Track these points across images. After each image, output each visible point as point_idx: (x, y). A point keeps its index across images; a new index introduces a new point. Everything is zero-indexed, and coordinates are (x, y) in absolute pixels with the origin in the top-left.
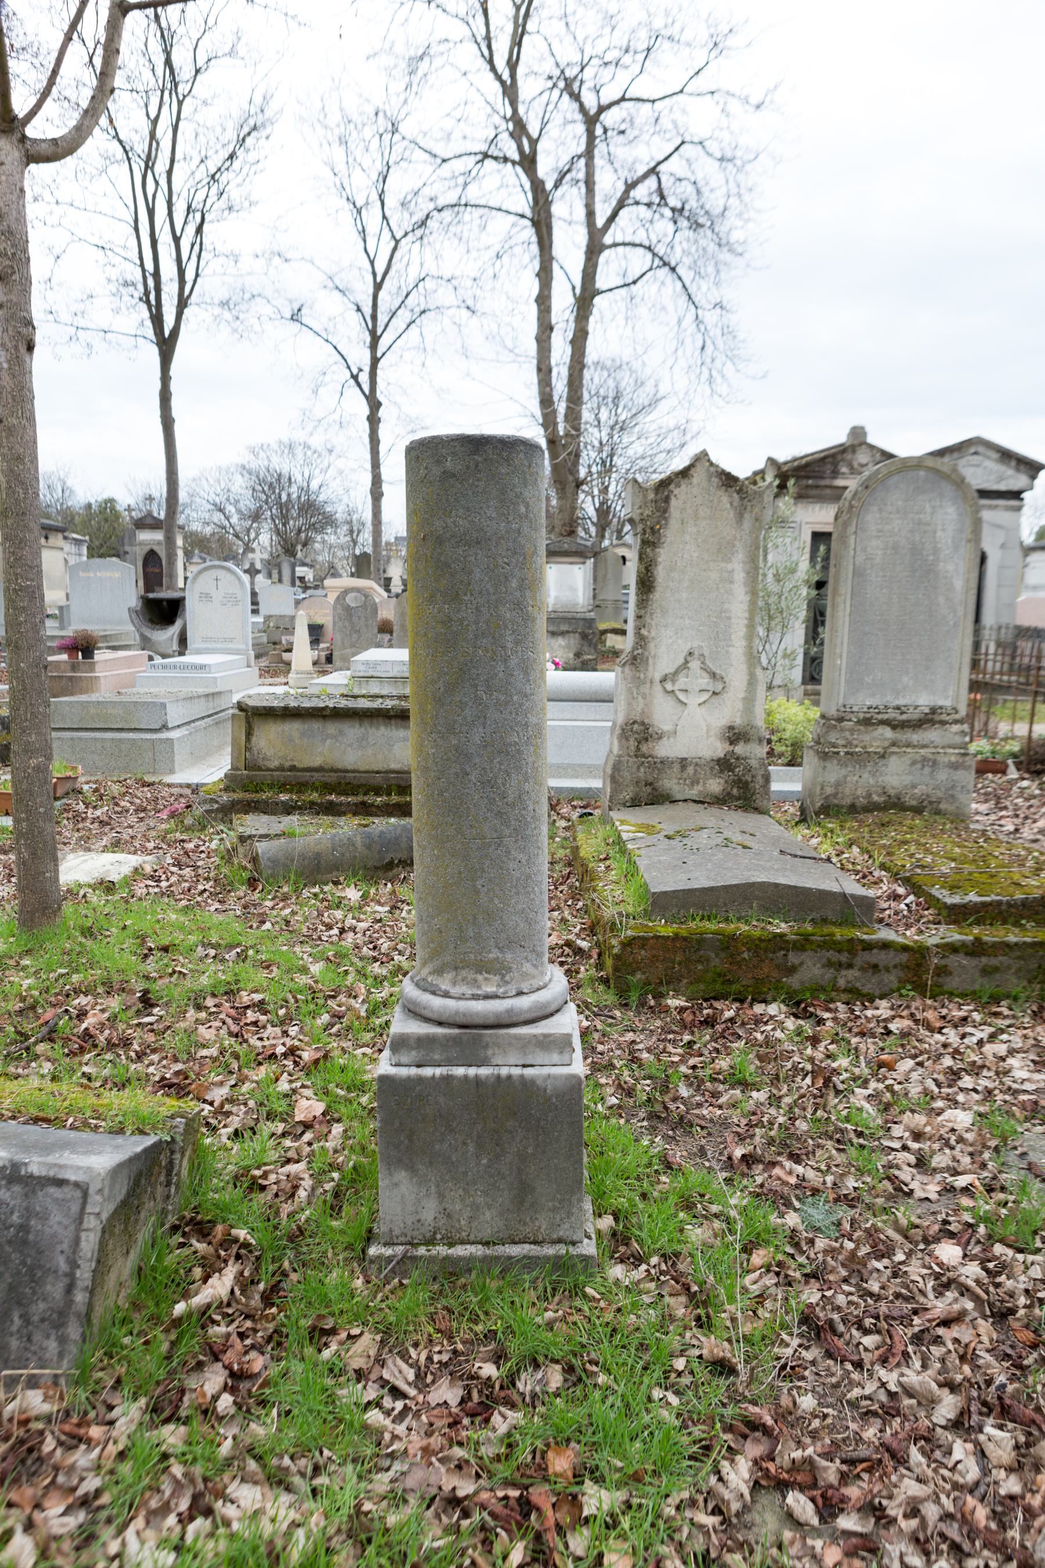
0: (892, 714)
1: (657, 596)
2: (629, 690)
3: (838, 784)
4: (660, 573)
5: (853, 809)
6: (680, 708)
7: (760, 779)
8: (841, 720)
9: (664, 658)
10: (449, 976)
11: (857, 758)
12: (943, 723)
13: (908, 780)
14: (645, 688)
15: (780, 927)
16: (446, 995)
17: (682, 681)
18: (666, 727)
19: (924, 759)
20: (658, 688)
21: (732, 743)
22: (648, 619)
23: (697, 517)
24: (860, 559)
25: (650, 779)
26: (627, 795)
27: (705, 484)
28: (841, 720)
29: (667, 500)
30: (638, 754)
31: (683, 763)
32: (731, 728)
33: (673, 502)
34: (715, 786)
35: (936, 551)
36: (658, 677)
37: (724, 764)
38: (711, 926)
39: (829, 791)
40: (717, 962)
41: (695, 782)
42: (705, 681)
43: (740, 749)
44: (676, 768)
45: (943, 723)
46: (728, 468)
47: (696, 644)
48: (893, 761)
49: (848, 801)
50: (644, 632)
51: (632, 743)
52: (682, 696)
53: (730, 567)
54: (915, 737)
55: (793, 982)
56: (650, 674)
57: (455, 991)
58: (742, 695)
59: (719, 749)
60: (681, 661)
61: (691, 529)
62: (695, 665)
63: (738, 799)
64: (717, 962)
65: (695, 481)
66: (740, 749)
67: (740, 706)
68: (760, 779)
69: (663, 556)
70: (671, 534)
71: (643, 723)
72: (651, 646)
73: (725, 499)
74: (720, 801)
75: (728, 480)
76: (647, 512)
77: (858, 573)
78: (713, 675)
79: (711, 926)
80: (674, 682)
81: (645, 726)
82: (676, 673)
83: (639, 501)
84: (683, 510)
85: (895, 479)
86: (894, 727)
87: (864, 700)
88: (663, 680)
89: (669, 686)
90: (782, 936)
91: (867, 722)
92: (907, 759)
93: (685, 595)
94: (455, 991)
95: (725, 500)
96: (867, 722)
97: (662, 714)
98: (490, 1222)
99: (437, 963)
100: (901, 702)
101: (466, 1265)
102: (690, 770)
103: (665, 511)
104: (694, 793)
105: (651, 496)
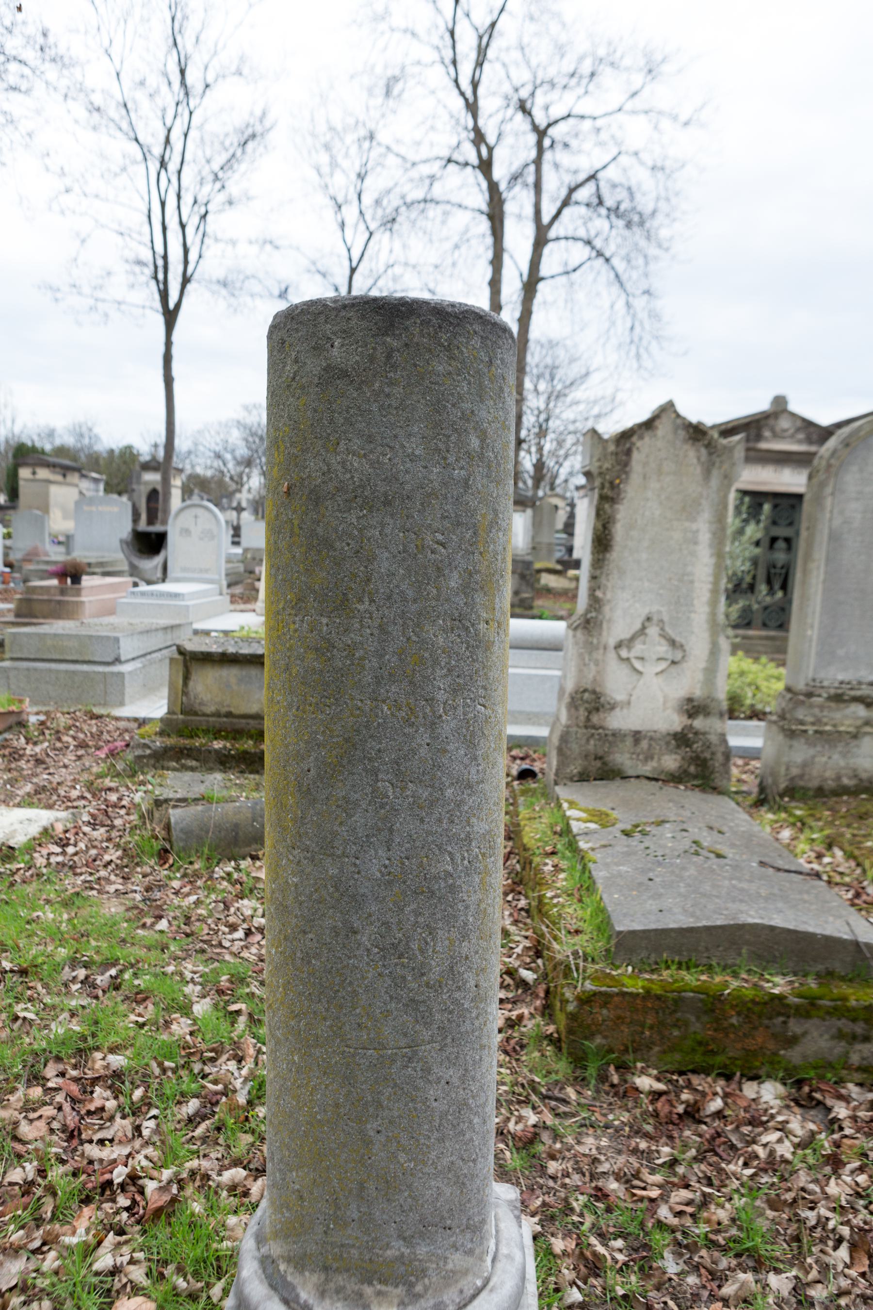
1: (614, 555)
2: (581, 656)
3: (805, 765)
4: (619, 531)
5: (820, 792)
6: (635, 677)
7: (720, 757)
8: (810, 695)
9: (620, 622)
11: (828, 738)
14: (598, 655)
15: (778, 985)
17: (639, 648)
20: (612, 655)
21: (690, 716)
22: (603, 580)
23: (660, 472)
24: (837, 522)
26: (574, 769)
28: (810, 695)
29: (629, 453)
30: (588, 724)
31: (637, 736)
32: (690, 700)
33: (636, 455)
34: (671, 762)
36: (612, 642)
37: (681, 739)
38: (691, 978)
39: (795, 771)
40: (698, 1028)
41: (649, 757)
42: (663, 649)
43: (698, 723)
44: (629, 741)
47: (655, 608)
49: (815, 784)
50: (599, 594)
51: (582, 713)
52: (638, 665)
53: (694, 527)
55: (794, 1055)
56: (604, 639)
58: (702, 665)
59: (675, 722)
61: (654, 485)
62: (653, 631)
63: (695, 777)
64: (698, 1028)
66: (698, 723)
67: (700, 676)
68: (720, 757)
69: (623, 513)
70: (631, 490)
71: (594, 692)
72: (606, 609)
73: (692, 454)
74: (676, 778)
75: (697, 433)
76: (607, 465)
77: (835, 538)
78: (673, 643)
79: (691, 978)
80: (629, 648)
81: (597, 695)
82: (632, 639)
83: (598, 452)
84: (646, 464)
87: (836, 675)
88: (619, 646)
89: (624, 653)
90: (781, 998)
91: (838, 698)
93: (644, 556)
95: (692, 455)
96: (838, 698)
97: (616, 682)
102: (644, 744)
103: (626, 464)
104: (647, 769)
105: (612, 448)
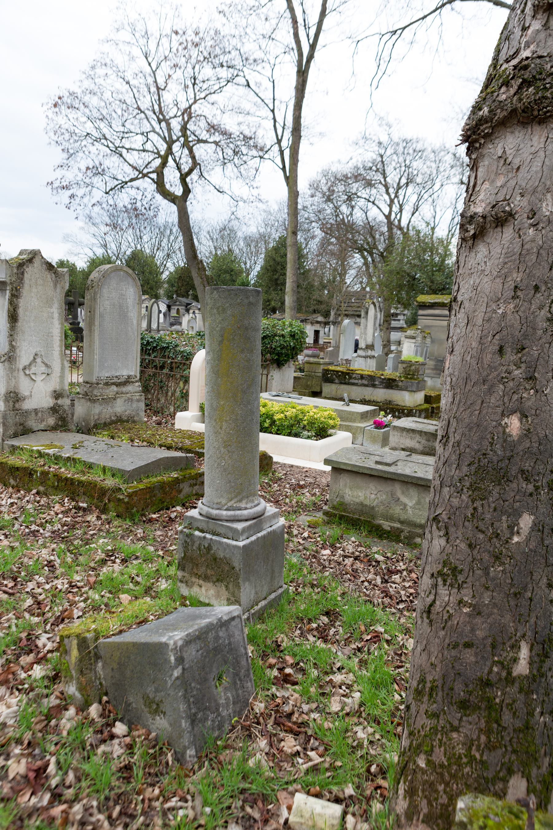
0: (115, 380)
1: (19, 324)
2: (7, 375)
3: (99, 414)
4: (21, 312)
5: (105, 424)
6: (32, 383)
7: (70, 416)
8: (98, 384)
10: (244, 501)
11: (107, 401)
12: (133, 382)
13: (123, 408)
14: (15, 374)
15: (175, 475)
16: (246, 509)
17: (33, 369)
18: (27, 393)
19: (129, 399)
20: (22, 373)
21: (57, 398)
22: (15, 337)
23: (36, 284)
24: (102, 309)
25: (22, 422)
26: (11, 432)
27: (40, 267)
28: (98, 384)
29: (23, 274)
30: (14, 409)
31: (36, 411)
32: (55, 391)
33: (26, 274)
34: (51, 421)
35: (127, 307)
36: (21, 367)
37: (54, 410)
38: (154, 480)
39: (96, 417)
40: (159, 495)
41: (42, 421)
42: (43, 369)
43: (60, 402)
44: (33, 414)
45: (133, 382)
46: (50, 260)
47: (38, 349)
48: (118, 400)
49: (103, 421)
50: (14, 343)
51: (11, 404)
52: (33, 377)
53: (52, 310)
54: (124, 389)
55: (181, 496)
56: (17, 366)
57: (249, 506)
58: (59, 375)
59: (49, 402)
60: (32, 358)
61: (34, 290)
62: (39, 360)
63: (61, 426)
64: (159, 495)
65: (35, 265)
66: (60, 402)
67: (58, 380)
68: (70, 416)
69: (22, 303)
70: (25, 291)
71: (15, 392)
72: (18, 351)
73: (49, 276)
74: (54, 429)
75: (50, 266)
76: (13, 279)
77: (101, 316)
78: (47, 365)
79: (154, 480)
80: (30, 369)
81: (16, 394)
82: (30, 365)
83: (9, 273)
84: (30, 280)
85: (113, 274)
86: (117, 386)
87: (105, 374)
88: (24, 369)
89: (27, 372)
90: (177, 478)
91: (107, 384)
92: (123, 400)
93: (32, 324)
94: (249, 506)
95: (49, 276)
96: (107, 384)
97: (24, 386)
98: (266, 589)
99: (239, 498)
100: (117, 374)
101: (264, 609)
102: (40, 414)
103: (22, 279)
104: (42, 426)
105: (15, 271)
